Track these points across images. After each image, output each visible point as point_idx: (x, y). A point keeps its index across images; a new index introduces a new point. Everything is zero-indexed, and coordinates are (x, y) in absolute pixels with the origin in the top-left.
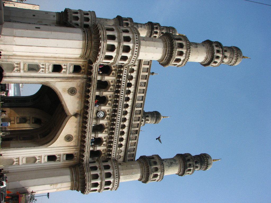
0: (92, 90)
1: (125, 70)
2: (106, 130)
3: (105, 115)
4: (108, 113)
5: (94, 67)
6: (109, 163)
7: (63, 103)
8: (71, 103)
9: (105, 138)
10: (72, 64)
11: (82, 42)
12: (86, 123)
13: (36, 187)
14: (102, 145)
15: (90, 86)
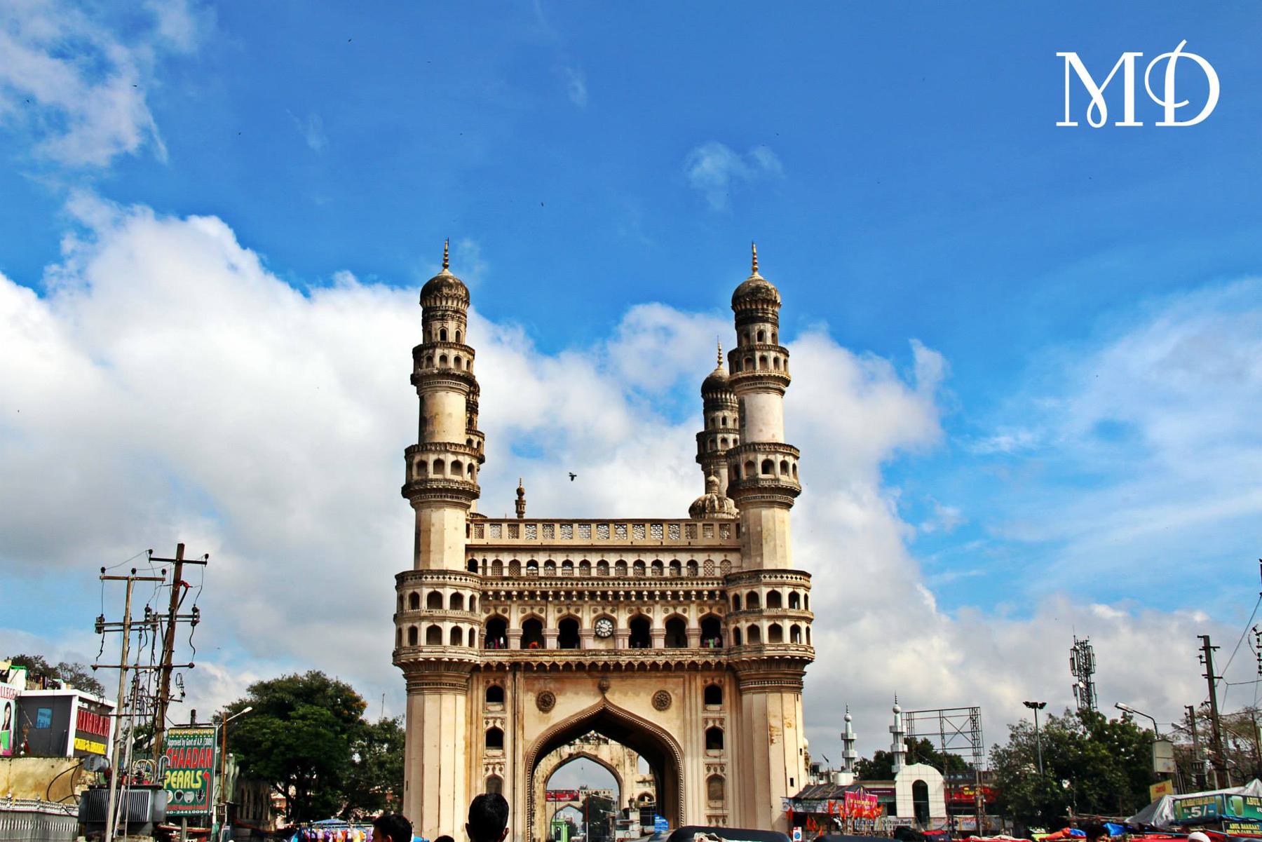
0: (539, 659)
1: (490, 588)
2: (644, 610)
3: (605, 617)
4: (600, 612)
5: (485, 660)
6: (731, 594)
7: (573, 720)
8: (574, 703)
9: (666, 611)
10: (485, 709)
11: (427, 697)
12: (618, 665)
13: (772, 777)
14: (686, 615)
15: (528, 665)
